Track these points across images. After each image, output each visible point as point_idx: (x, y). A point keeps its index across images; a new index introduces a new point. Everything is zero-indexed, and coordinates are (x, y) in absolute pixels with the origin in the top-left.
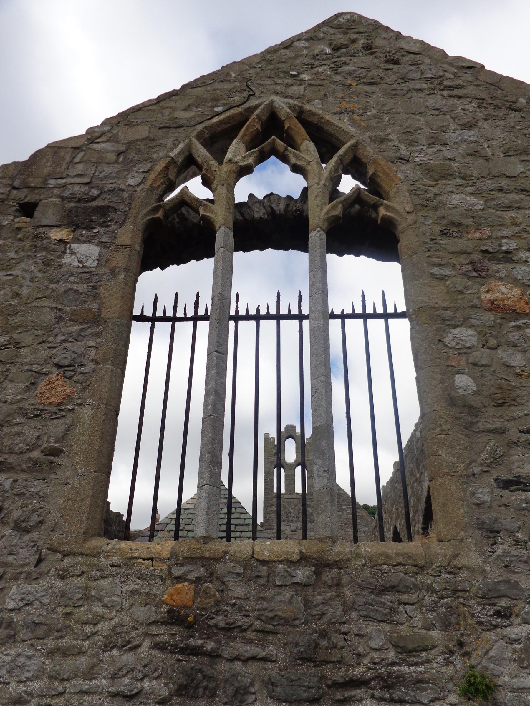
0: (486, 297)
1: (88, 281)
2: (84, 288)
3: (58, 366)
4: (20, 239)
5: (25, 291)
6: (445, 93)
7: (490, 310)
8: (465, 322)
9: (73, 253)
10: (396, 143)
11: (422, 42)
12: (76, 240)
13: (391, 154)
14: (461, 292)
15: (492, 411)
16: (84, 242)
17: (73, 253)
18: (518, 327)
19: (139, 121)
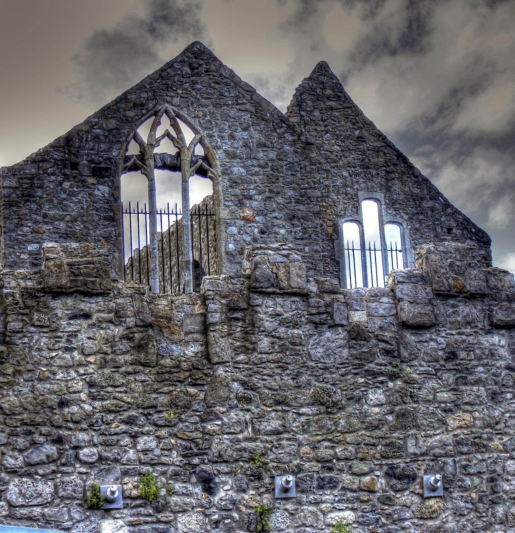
0: (242, 214)
1: (108, 203)
2: (106, 206)
3: (104, 238)
4: (76, 182)
5: (85, 207)
6: (238, 107)
7: (243, 219)
8: (235, 224)
9: (99, 190)
10: (216, 138)
11: (232, 71)
12: (98, 183)
13: (214, 144)
14: (234, 212)
15: (238, 256)
16: (102, 185)
17: (99, 190)
18: (250, 227)
19: (110, 116)
